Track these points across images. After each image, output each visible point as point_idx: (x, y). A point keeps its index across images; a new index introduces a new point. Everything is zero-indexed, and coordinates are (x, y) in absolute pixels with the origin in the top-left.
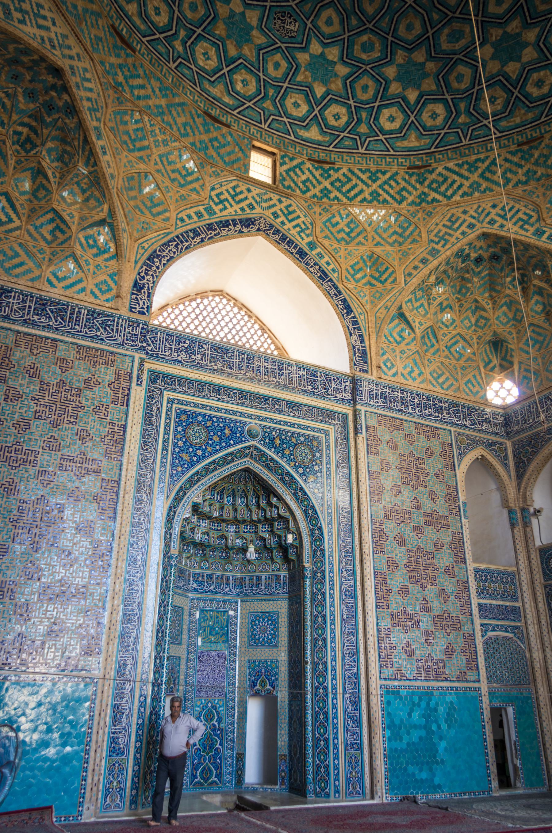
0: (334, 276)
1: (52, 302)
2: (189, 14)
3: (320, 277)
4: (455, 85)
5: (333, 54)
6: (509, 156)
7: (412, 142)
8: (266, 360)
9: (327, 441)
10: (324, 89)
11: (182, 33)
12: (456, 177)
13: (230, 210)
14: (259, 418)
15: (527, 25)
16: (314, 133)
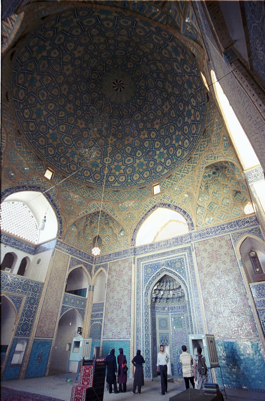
0: (179, 206)
1: (117, 253)
2: (129, 173)
3: (175, 209)
4: (186, 132)
5: (162, 150)
6: (203, 140)
7: (186, 154)
8: (163, 242)
9: (185, 257)
10: (164, 159)
11: (129, 178)
12: (196, 156)
13: (150, 207)
14: (164, 259)
15: (188, 106)
16: (166, 171)
